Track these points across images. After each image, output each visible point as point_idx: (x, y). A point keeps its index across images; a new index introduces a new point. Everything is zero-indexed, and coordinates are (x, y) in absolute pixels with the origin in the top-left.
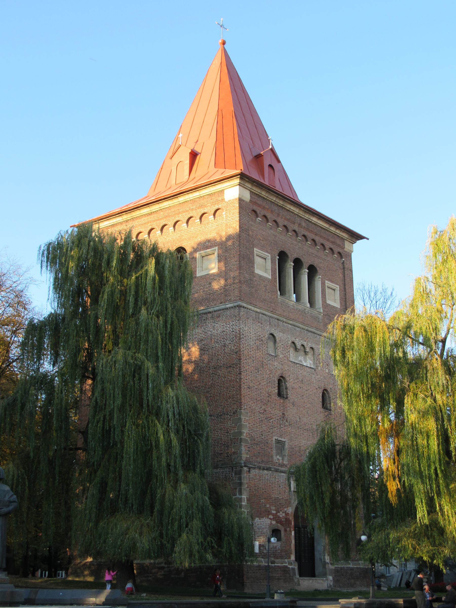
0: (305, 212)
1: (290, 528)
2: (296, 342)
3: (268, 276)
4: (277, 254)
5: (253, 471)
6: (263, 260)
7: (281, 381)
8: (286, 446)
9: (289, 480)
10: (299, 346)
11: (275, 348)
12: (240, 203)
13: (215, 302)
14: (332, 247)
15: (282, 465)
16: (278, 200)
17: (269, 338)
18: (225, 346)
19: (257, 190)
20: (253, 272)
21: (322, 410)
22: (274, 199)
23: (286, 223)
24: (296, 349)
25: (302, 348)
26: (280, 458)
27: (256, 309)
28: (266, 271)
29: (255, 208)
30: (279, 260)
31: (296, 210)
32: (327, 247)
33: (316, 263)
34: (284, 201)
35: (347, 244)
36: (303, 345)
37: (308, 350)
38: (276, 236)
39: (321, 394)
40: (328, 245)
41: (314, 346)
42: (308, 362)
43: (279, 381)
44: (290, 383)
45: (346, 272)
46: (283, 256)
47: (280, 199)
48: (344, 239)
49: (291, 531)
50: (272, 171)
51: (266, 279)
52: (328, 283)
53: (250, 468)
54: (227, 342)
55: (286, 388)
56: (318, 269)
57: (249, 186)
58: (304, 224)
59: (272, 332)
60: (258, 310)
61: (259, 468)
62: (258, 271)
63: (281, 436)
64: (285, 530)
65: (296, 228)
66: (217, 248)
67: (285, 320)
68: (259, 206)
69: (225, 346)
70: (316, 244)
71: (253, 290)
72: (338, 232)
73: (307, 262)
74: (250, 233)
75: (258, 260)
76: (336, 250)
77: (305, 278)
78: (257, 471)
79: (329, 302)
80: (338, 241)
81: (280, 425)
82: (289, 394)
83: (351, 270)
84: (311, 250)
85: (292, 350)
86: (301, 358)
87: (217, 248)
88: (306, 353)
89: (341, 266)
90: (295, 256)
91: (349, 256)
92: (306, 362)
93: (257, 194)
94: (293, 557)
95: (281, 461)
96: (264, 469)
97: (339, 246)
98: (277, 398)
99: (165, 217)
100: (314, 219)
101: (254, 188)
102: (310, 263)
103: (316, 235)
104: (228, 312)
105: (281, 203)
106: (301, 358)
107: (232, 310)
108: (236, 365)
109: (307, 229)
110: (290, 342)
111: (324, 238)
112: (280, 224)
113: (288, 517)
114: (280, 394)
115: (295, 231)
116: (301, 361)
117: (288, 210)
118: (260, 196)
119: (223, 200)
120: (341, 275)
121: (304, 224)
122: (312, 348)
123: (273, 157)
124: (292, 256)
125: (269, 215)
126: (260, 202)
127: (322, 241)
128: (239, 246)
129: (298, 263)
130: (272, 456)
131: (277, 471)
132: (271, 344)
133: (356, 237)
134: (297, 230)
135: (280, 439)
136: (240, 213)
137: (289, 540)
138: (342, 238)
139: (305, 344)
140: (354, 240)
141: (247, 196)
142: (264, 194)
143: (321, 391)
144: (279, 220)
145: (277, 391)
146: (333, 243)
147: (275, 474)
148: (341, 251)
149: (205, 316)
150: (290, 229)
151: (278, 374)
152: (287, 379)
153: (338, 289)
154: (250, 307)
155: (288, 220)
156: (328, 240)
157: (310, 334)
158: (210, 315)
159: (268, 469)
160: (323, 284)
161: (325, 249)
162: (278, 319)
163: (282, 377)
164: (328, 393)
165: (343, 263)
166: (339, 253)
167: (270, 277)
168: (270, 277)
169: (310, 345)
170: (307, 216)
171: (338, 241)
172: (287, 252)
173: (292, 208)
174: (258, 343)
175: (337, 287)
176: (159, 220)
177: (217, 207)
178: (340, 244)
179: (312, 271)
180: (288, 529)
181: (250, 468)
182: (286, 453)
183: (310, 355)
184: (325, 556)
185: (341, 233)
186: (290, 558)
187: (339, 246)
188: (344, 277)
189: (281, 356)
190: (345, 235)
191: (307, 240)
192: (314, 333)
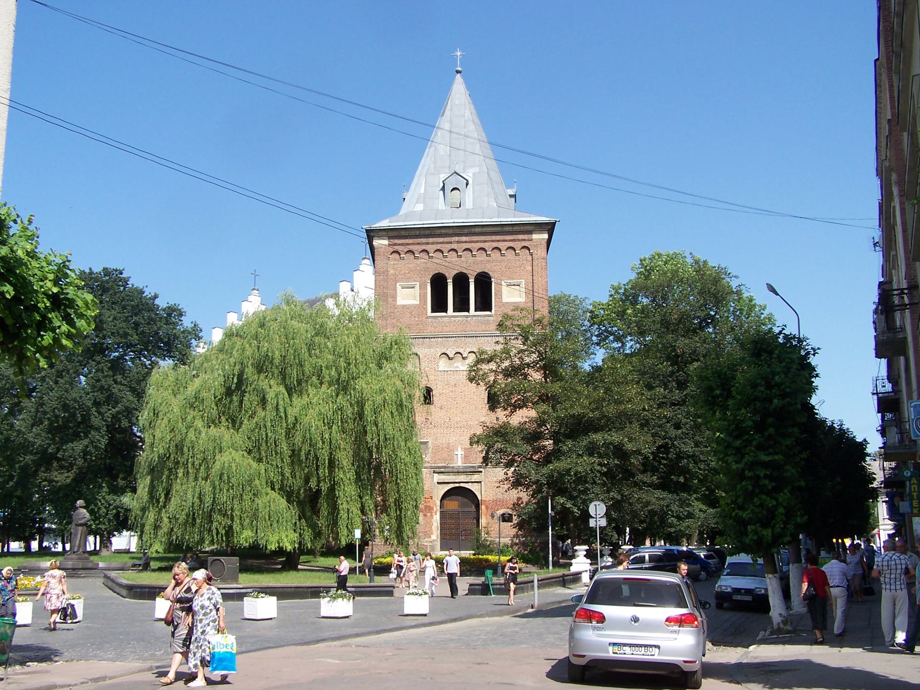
22: (418, 232)
29: (396, 248)
48: (532, 231)
49: (432, 516)
56: (490, 273)
58: (464, 239)
64: (425, 515)
89: (530, 258)
94: (434, 537)
113: (428, 504)
116: (457, 367)
139: (461, 351)
153: (524, 283)
170: (466, 231)
180: (429, 514)
185: (521, 228)
186: (430, 537)
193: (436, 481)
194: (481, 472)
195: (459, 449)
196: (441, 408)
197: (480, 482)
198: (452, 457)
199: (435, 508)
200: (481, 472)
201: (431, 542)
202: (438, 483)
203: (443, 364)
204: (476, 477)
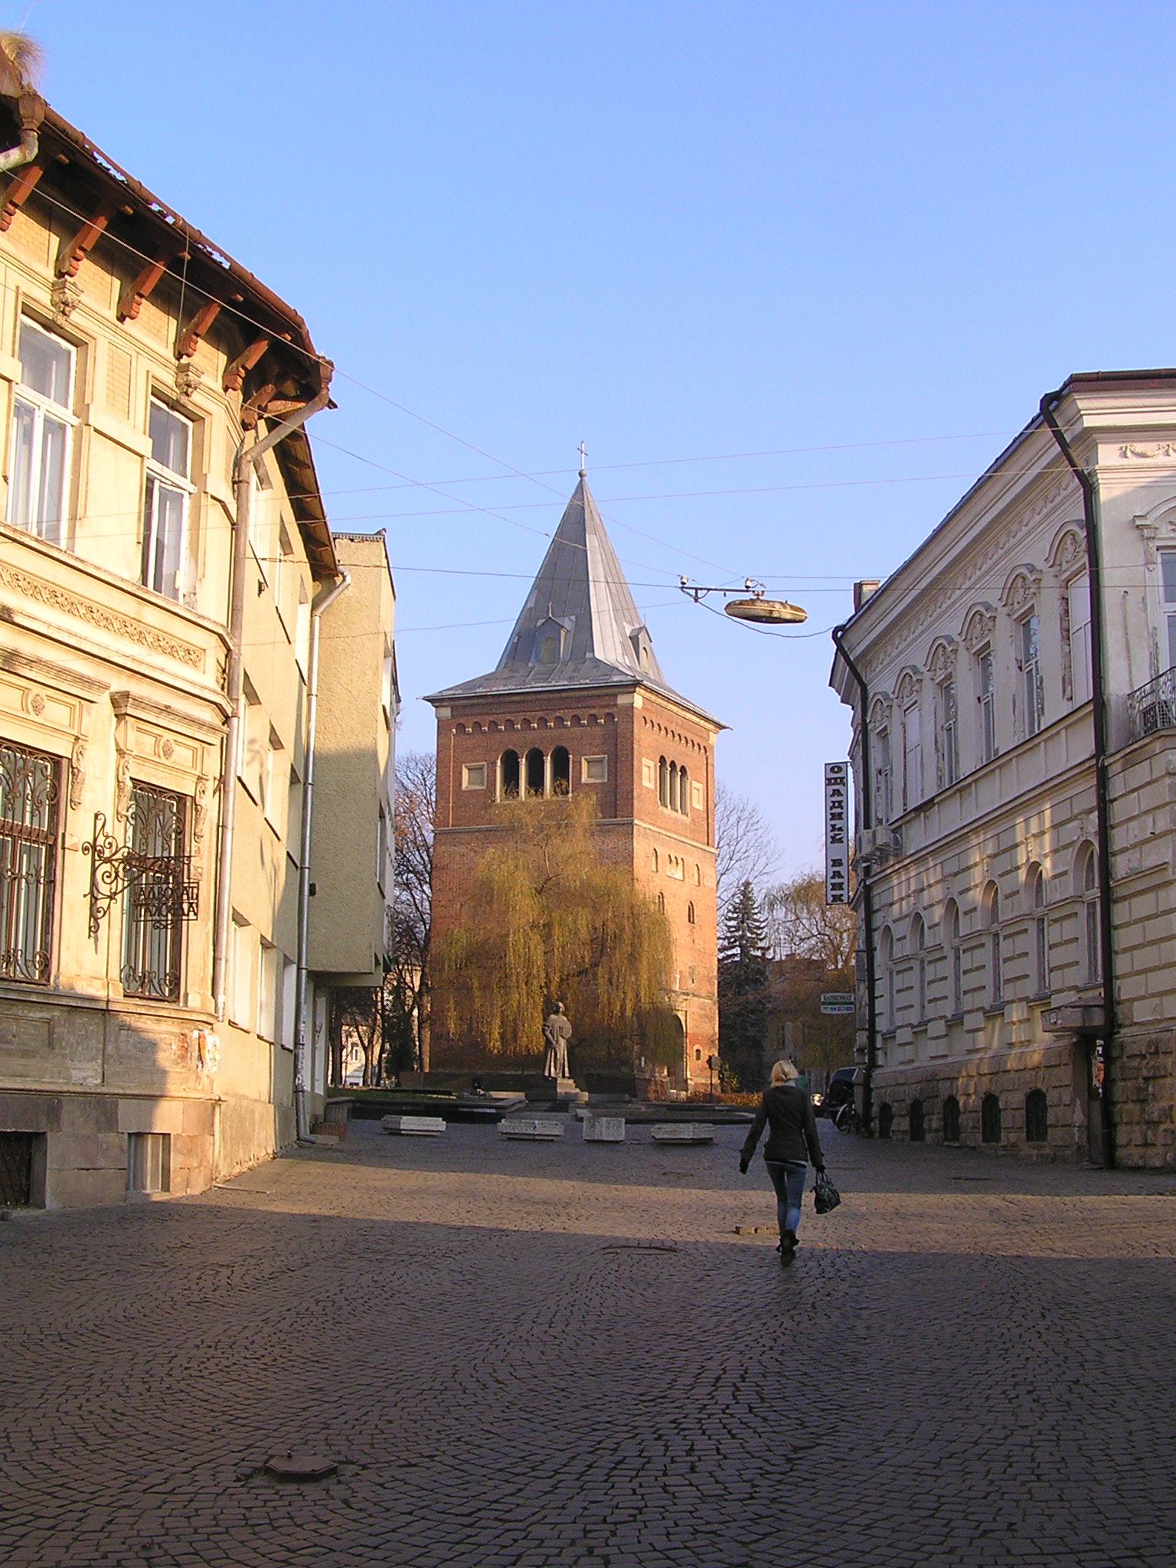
3: (651, 786)
4: (658, 761)
10: (673, 859)
19: (648, 695)
30: (660, 767)
46: (662, 759)
51: (650, 789)
66: (606, 756)
86: (673, 871)
87: (606, 756)
119: (616, 705)
142: (653, 697)
148: (705, 744)
178: (706, 736)
190: (711, 727)
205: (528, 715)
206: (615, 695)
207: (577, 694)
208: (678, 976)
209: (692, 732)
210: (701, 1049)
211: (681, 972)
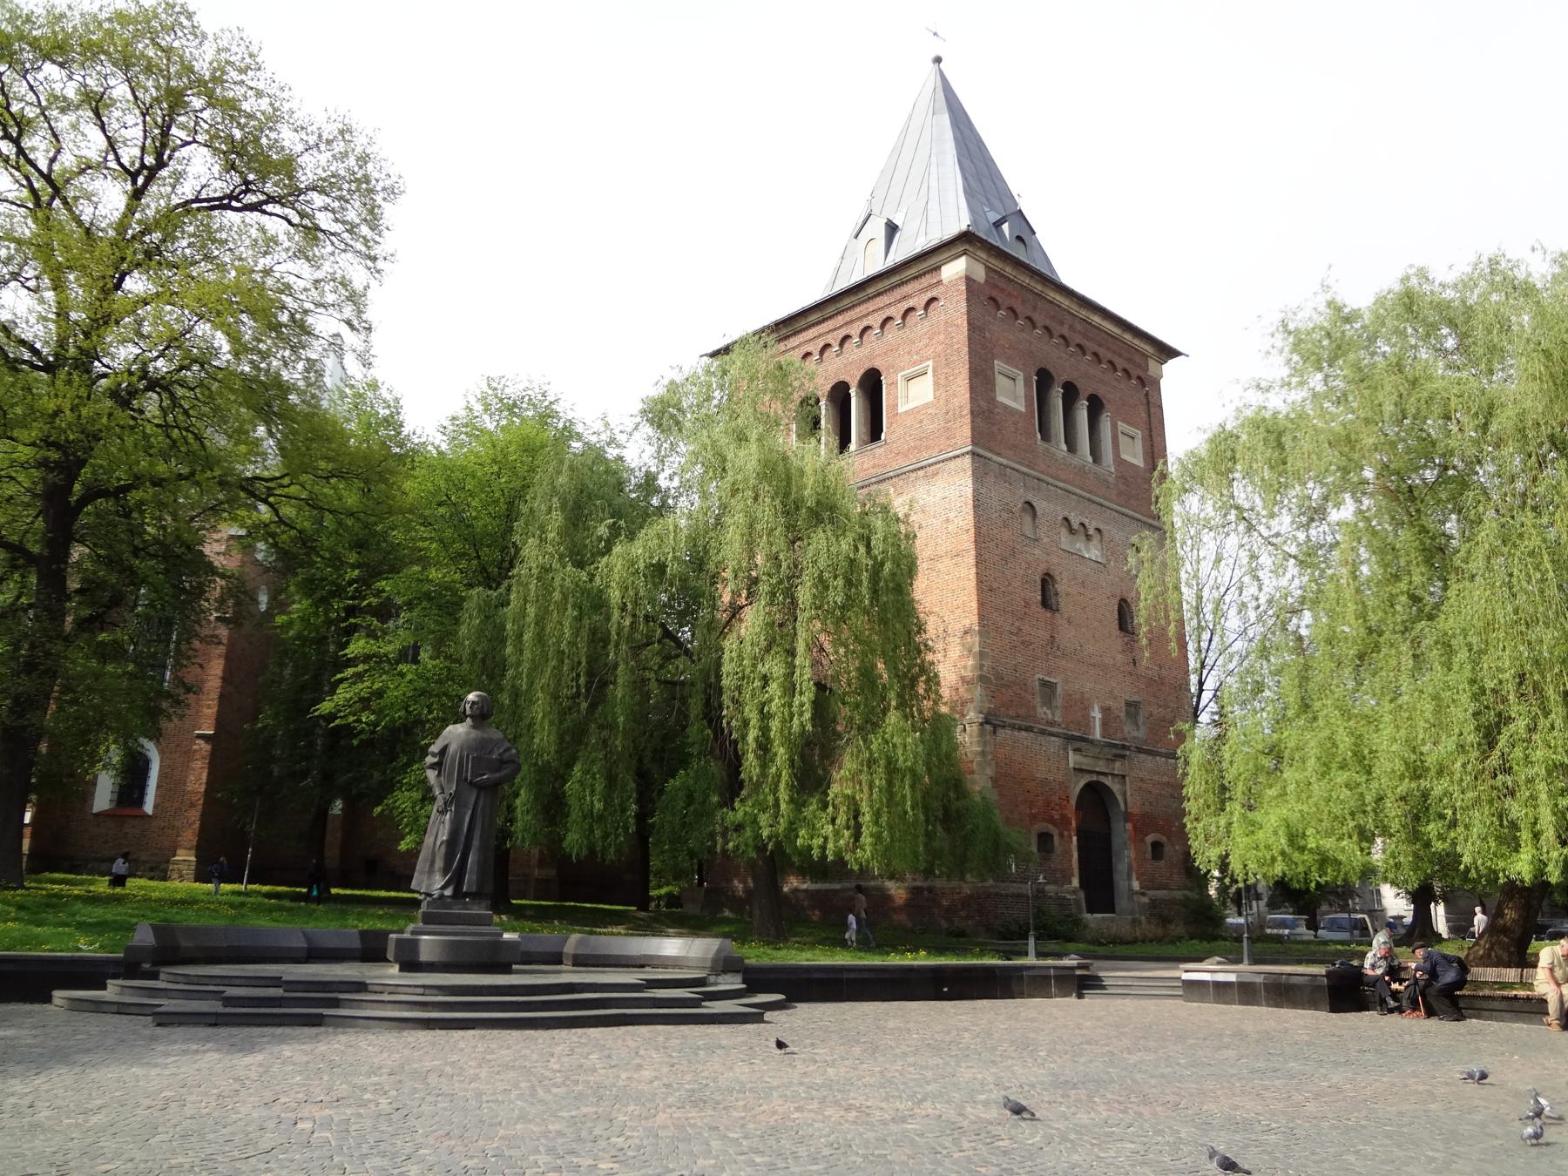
0: (1081, 306)
1: (1069, 830)
2: (1070, 518)
5: (1000, 731)
6: (1011, 382)
7: (1047, 581)
8: (1059, 690)
9: (1065, 749)
10: (1075, 525)
11: (1035, 527)
12: (967, 284)
13: (930, 451)
14: (1127, 367)
15: (1052, 724)
16: (1033, 284)
17: (1023, 510)
18: (948, 521)
19: (997, 264)
20: (993, 399)
21: (1118, 632)
23: (1048, 323)
24: (1071, 531)
25: (1082, 529)
26: (1048, 712)
27: (999, 459)
28: (1015, 399)
29: (995, 293)
31: (1065, 302)
32: (1119, 367)
33: (1101, 392)
34: (1044, 284)
35: (1152, 364)
36: (1082, 524)
37: (1091, 532)
38: (1031, 343)
39: (1116, 607)
40: (1120, 363)
41: (1101, 527)
42: (1093, 552)
43: (1044, 582)
44: (1062, 586)
45: (1152, 410)
46: (1044, 380)
47: (1038, 281)
50: (1022, 246)
52: (1122, 426)
53: (995, 727)
54: (951, 515)
55: (1057, 594)
57: (984, 256)
58: (1078, 326)
59: (1030, 498)
60: (1004, 461)
61: (1013, 727)
62: (1001, 398)
63: (1049, 674)
64: (1061, 835)
65: (1065, 331)
66: (930, 363)
67: (1050, 480)
68: (1002, 290)
69: (948, 521)
70: (1100, 361)
71: (995, 429)
72: (1137, 342)
73: (1085, 388)
74: (987, 335)
75: (1001, 381)
76: (1135, 372)
77: (1082, 416)
78: (1008, 731)
79: (1124, 456)
80: (1137, 358)
81: (1047, 654)
82: (1062, 602)
83: (1161, 407)
84: (1091, 371)
85: (1064, 532)
87: (930, 363)
88: (1088, 537)
90: (1065, 378)
91: (1156, 384)
92: (1088, 551)
93: (996, 272)
94: (1076, 882)
95: (1050, 716)
96: (1020, 729)
97: (1139, 366)
98: (1041, 610)
99: (846, 324)
100: (1096, 319)
101: (992, 260)
102: (1090, 391)
103: (1100, 345)
104: (952, 464)
105: (1039, 287)
106: (1080, 546)
107: (958, 461)
108: (967, 551)
109: (1085, 336)
110: (1060, 518)
111: (1114, 352)
112: (1039, 324)
114: (1045, 603)
115: (1063, 337)
116: (1080, 550)
117: (1051, 302)
118: (1003, 276)
119: (940, 282)
120: (1144, 415)
121: (1078, 326)
122: (1098, 530)
123: (1024, 223)
124: (1061, 377)
125: (1019, 308)
126: (1002, 283)
127: (1110, 356)
128: (970, 352)
129: (1071, 393)
130: (1034, 708)
131: (1043, 732)
132: (1028, 519)
133: (1168, 353)
134: (1067, 335)
135: (1047, 678)
136: (968, 300)
137: (1068, 853)
138: (1143, 354)
139: (1086, 522)
140: (1164, 357)
141: (980, 274)
142: (1009, 270)
143: (1115, 602)
144: (1036, 317)
145: (1039, 598)
146: (1129, 360)
147: (1041, 738)
148: (1141, 374)
149: (914, 475)
150: (1056, 334)
151: (1042, 569)
152: (1058, 578)
154: (989, 455)
155: (1052, 318)
156: (1120, 356)
157: (1094, 506)
158: (921, 473)
159: (1028, 729)
160: (1114, 427)
161: (1115, 370)
162: (1039, 479)
163: (1047, 574)
164: (1128, 606)
165: (1147, 395)
166: (1139, 378)
167: (1023, 410)
168: (1023, 410)
169: (1094, 524)
170: (1084, 313)
171: (1137, 358)
172: (1052, 371)
173: (1059, 298)
174: (1005, 515)
175: (1139, 434)
176: (835, 329)
177: (929, 295)
179: (1096, 406)
180: (1066, 833)
181: (995, 727)
182: (1059, 702)
183: (1096, 538)
184: (1130, 878)
186: (1070, 883)
187: (1139, 366)
188: (1149, 416)
189: (1046, 540)
190: (1148, 349)
191: (1084, 354)
192: (1102, 505)
193: (1071, 765)
194: (1123, 757)
195: (1097, 708)
196: (1070, 622)
197: (1124, 777)
198: (1086, 722)
199: (1074, 823)
200: (1123, 757)
201: (1074, 892)
202: (1075, 769)
203: (1064, 539)
204: (1118, 767)
205: (829, 339)
206: (938, 268)
207: (886, 283)
208: (1097, 714)
209: (1108, 349)
210: (1164, 839)
211: (1106, 711)
